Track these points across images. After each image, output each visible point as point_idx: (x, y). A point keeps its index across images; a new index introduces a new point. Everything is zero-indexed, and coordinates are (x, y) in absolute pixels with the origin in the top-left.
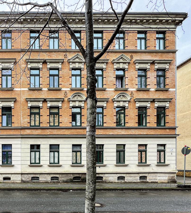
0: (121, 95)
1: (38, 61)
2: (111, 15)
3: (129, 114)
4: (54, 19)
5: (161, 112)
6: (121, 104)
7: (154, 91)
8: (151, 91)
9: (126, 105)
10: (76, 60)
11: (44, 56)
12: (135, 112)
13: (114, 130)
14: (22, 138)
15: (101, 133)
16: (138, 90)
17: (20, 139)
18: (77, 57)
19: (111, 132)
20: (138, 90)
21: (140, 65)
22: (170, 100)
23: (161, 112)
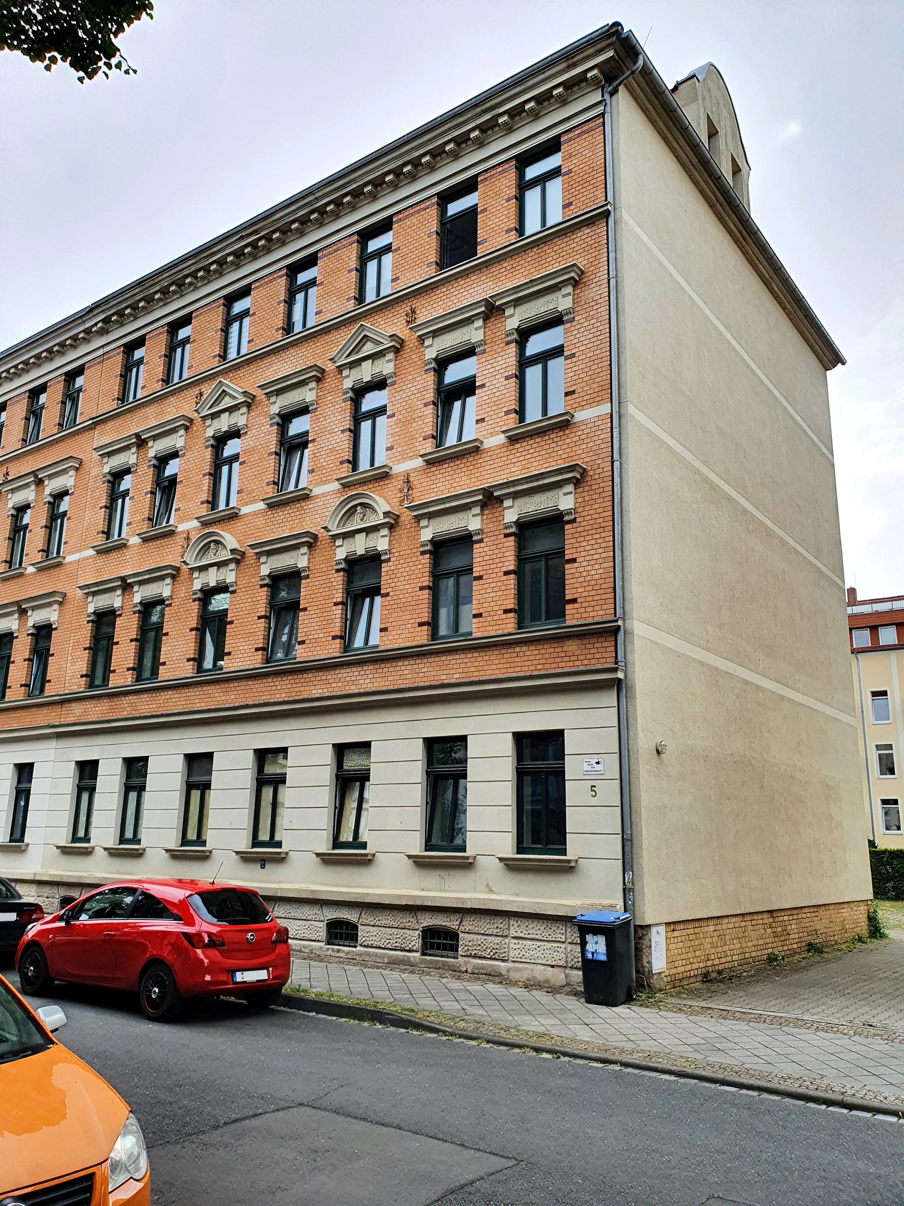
0: (356, 506)
1: (161, 430)
2: (317, 195)
3: (392, 585)
4: (171, 285)
5: (541, 548)
6: (360, 546)
7: (35, 573)
8: (489, 450)
9: (381, 542)
10: (365, 348)
11: (147, 418)
12: (416, 572)
13: (330, 676)
14: (59, 736)
15: (284, 695)
16: (432, 462)
17: (53, 744)
18: (365, 336)
19: (317, 687)
20: (432, 462)
21: (520, 309)
22: (577, 477)
23: (541, 548)
